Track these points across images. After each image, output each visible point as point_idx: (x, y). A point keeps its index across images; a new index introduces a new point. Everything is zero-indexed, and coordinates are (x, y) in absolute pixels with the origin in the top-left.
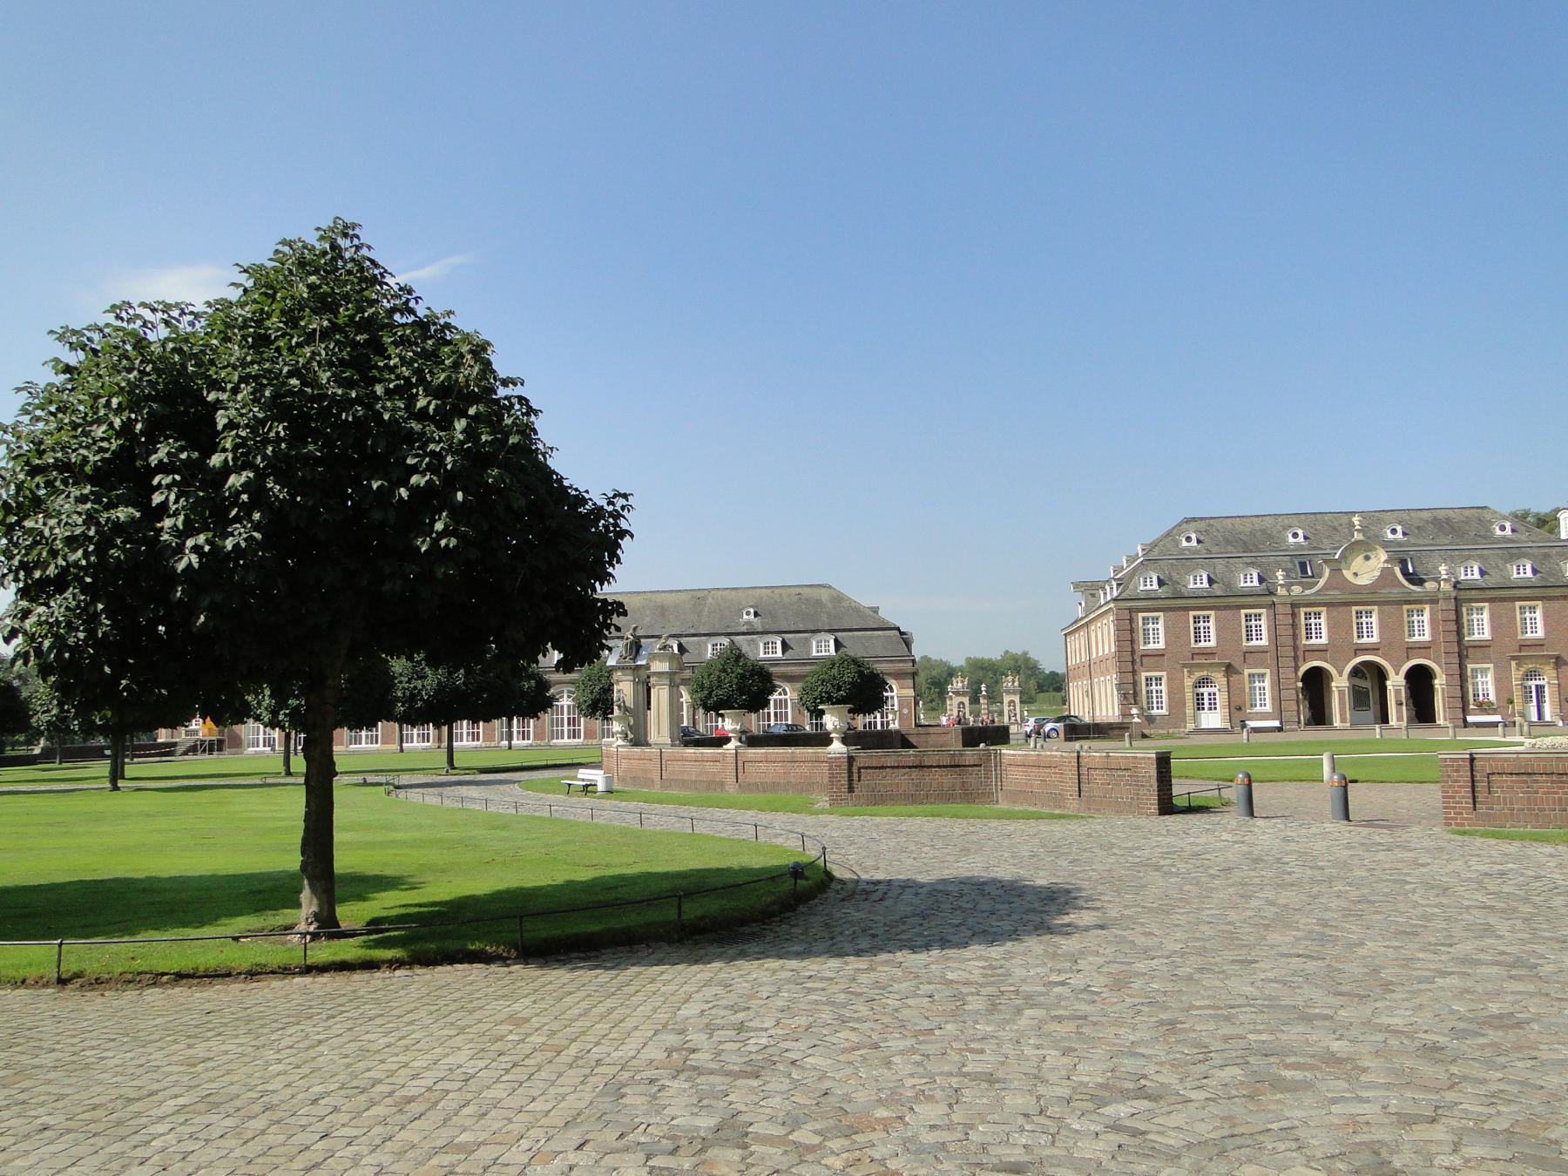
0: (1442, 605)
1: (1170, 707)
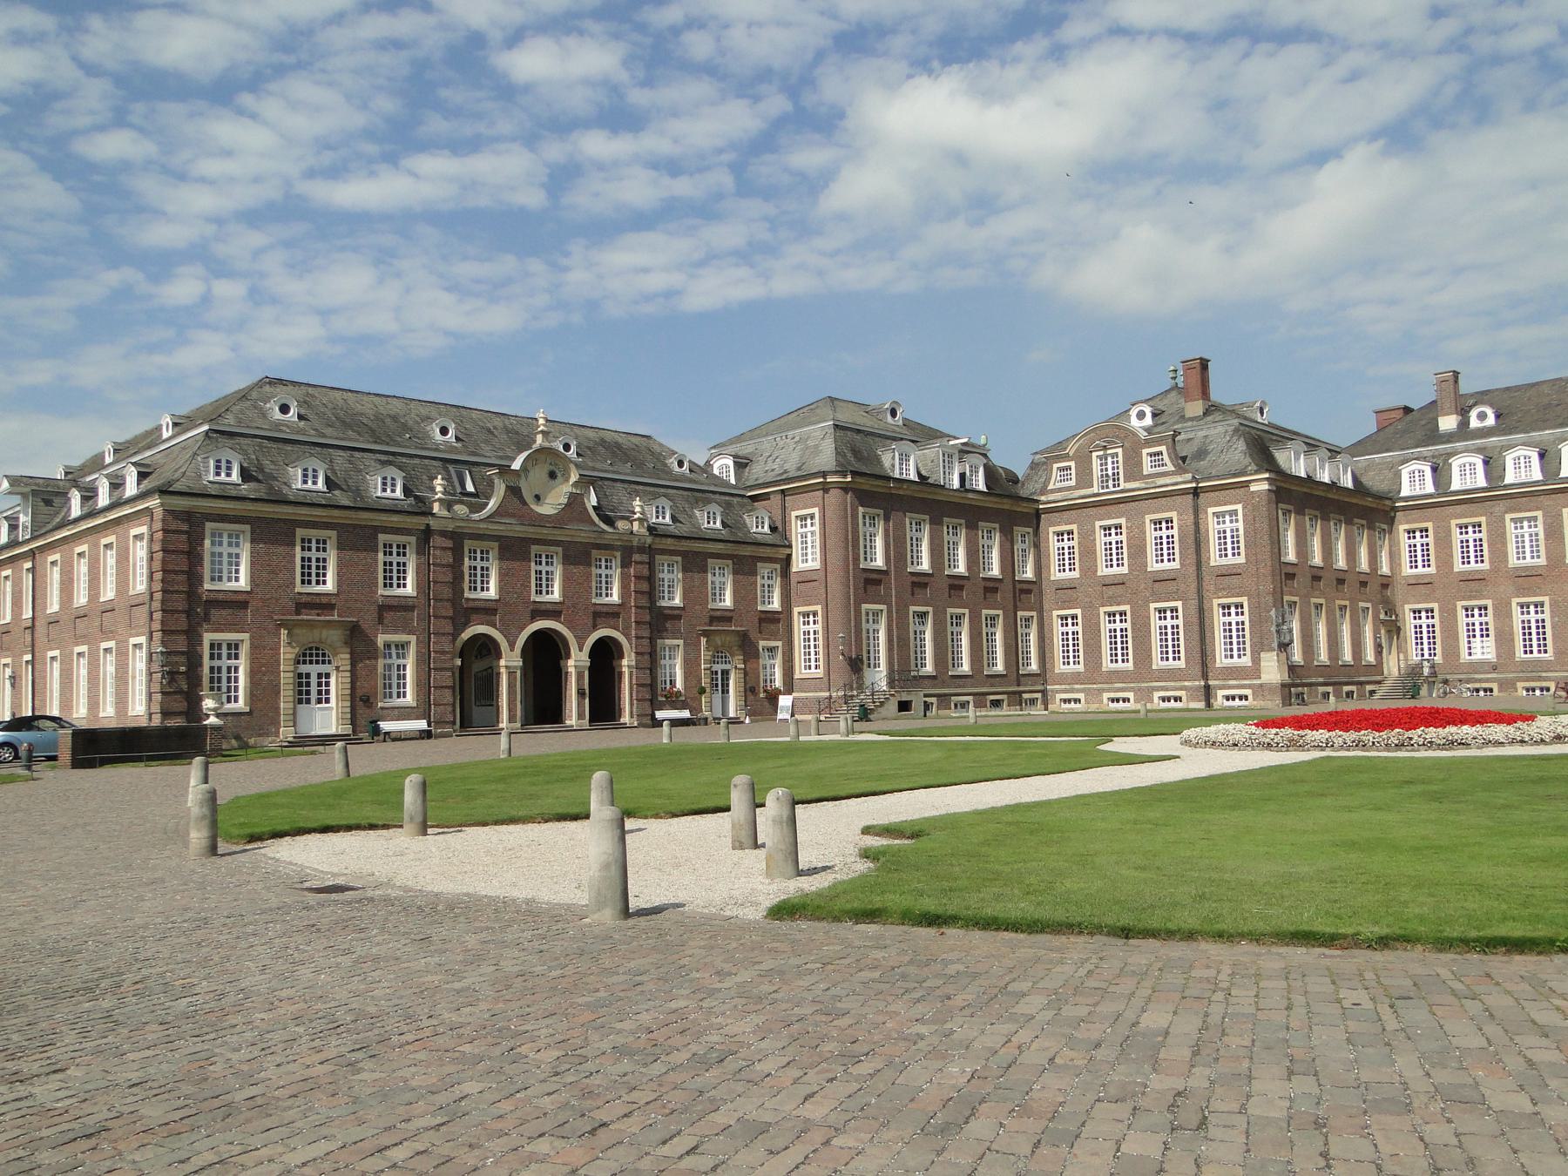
1: (252, 696)
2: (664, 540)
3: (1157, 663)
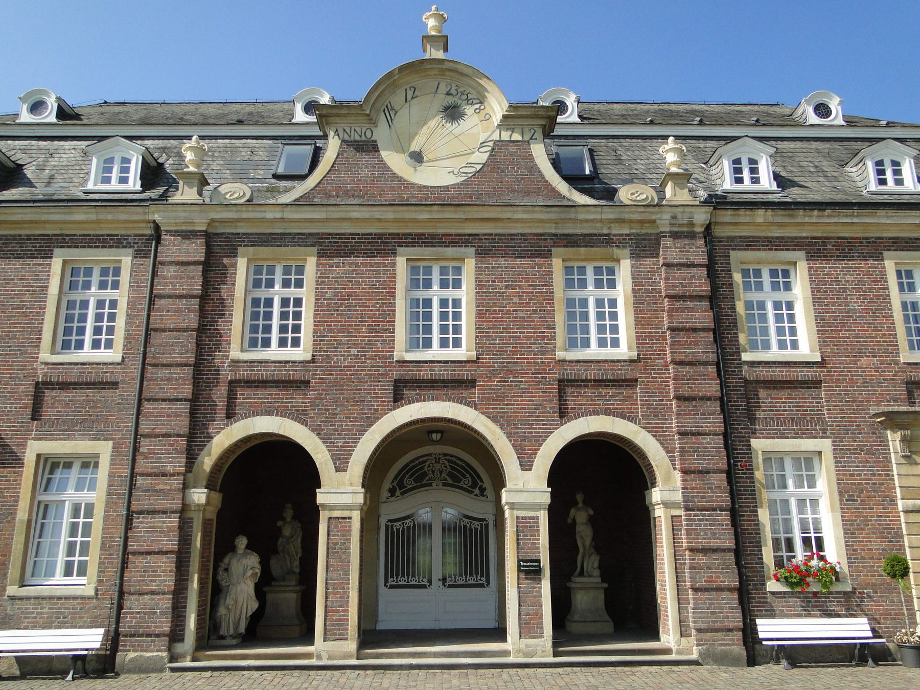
0: (671, 251)
2: (744, 216)
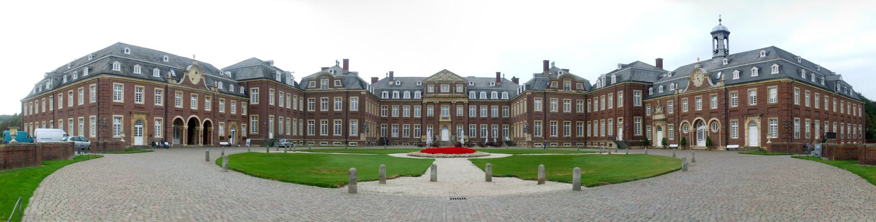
3: (335, 135)
